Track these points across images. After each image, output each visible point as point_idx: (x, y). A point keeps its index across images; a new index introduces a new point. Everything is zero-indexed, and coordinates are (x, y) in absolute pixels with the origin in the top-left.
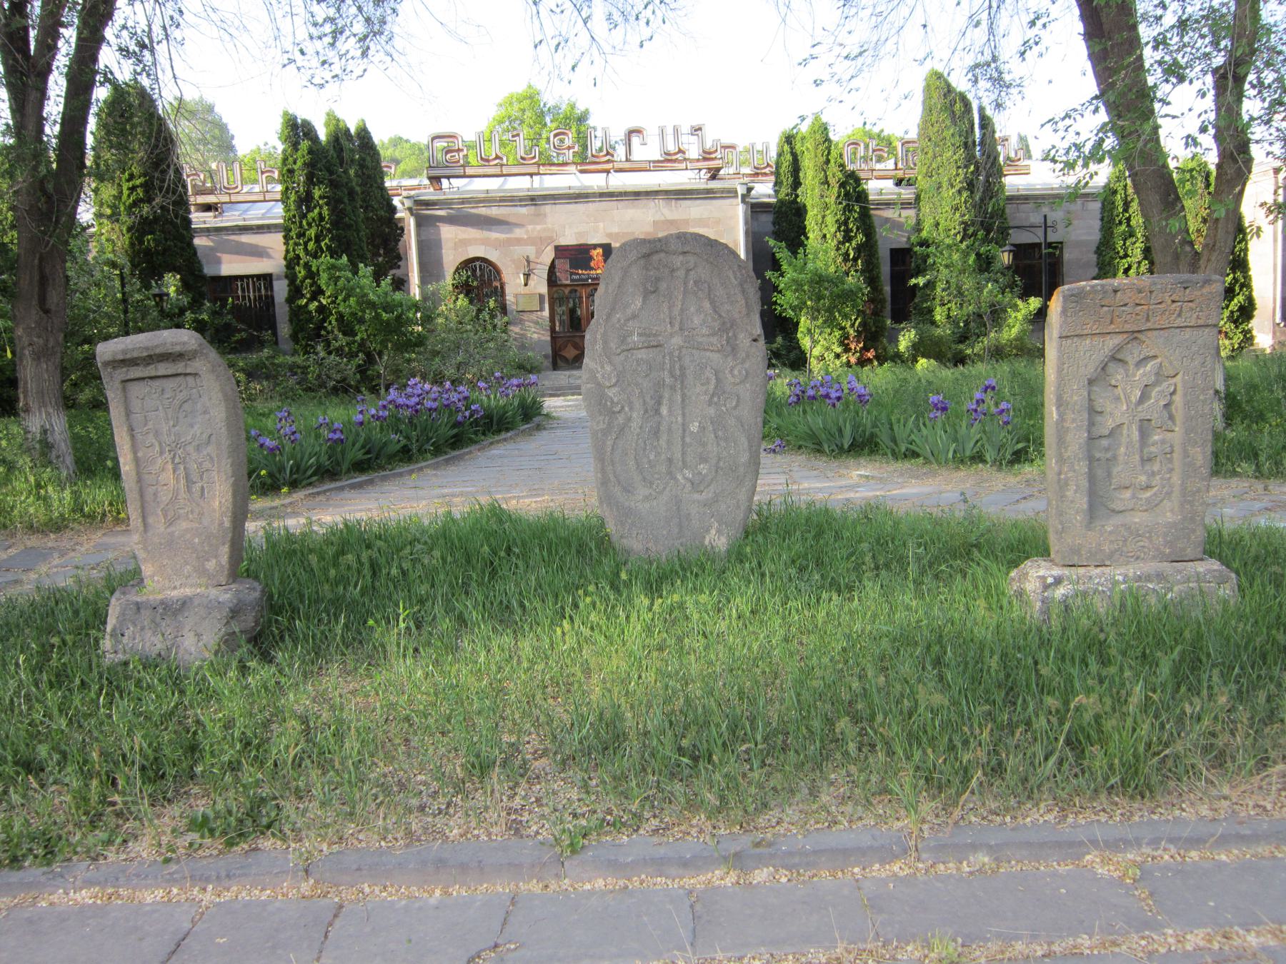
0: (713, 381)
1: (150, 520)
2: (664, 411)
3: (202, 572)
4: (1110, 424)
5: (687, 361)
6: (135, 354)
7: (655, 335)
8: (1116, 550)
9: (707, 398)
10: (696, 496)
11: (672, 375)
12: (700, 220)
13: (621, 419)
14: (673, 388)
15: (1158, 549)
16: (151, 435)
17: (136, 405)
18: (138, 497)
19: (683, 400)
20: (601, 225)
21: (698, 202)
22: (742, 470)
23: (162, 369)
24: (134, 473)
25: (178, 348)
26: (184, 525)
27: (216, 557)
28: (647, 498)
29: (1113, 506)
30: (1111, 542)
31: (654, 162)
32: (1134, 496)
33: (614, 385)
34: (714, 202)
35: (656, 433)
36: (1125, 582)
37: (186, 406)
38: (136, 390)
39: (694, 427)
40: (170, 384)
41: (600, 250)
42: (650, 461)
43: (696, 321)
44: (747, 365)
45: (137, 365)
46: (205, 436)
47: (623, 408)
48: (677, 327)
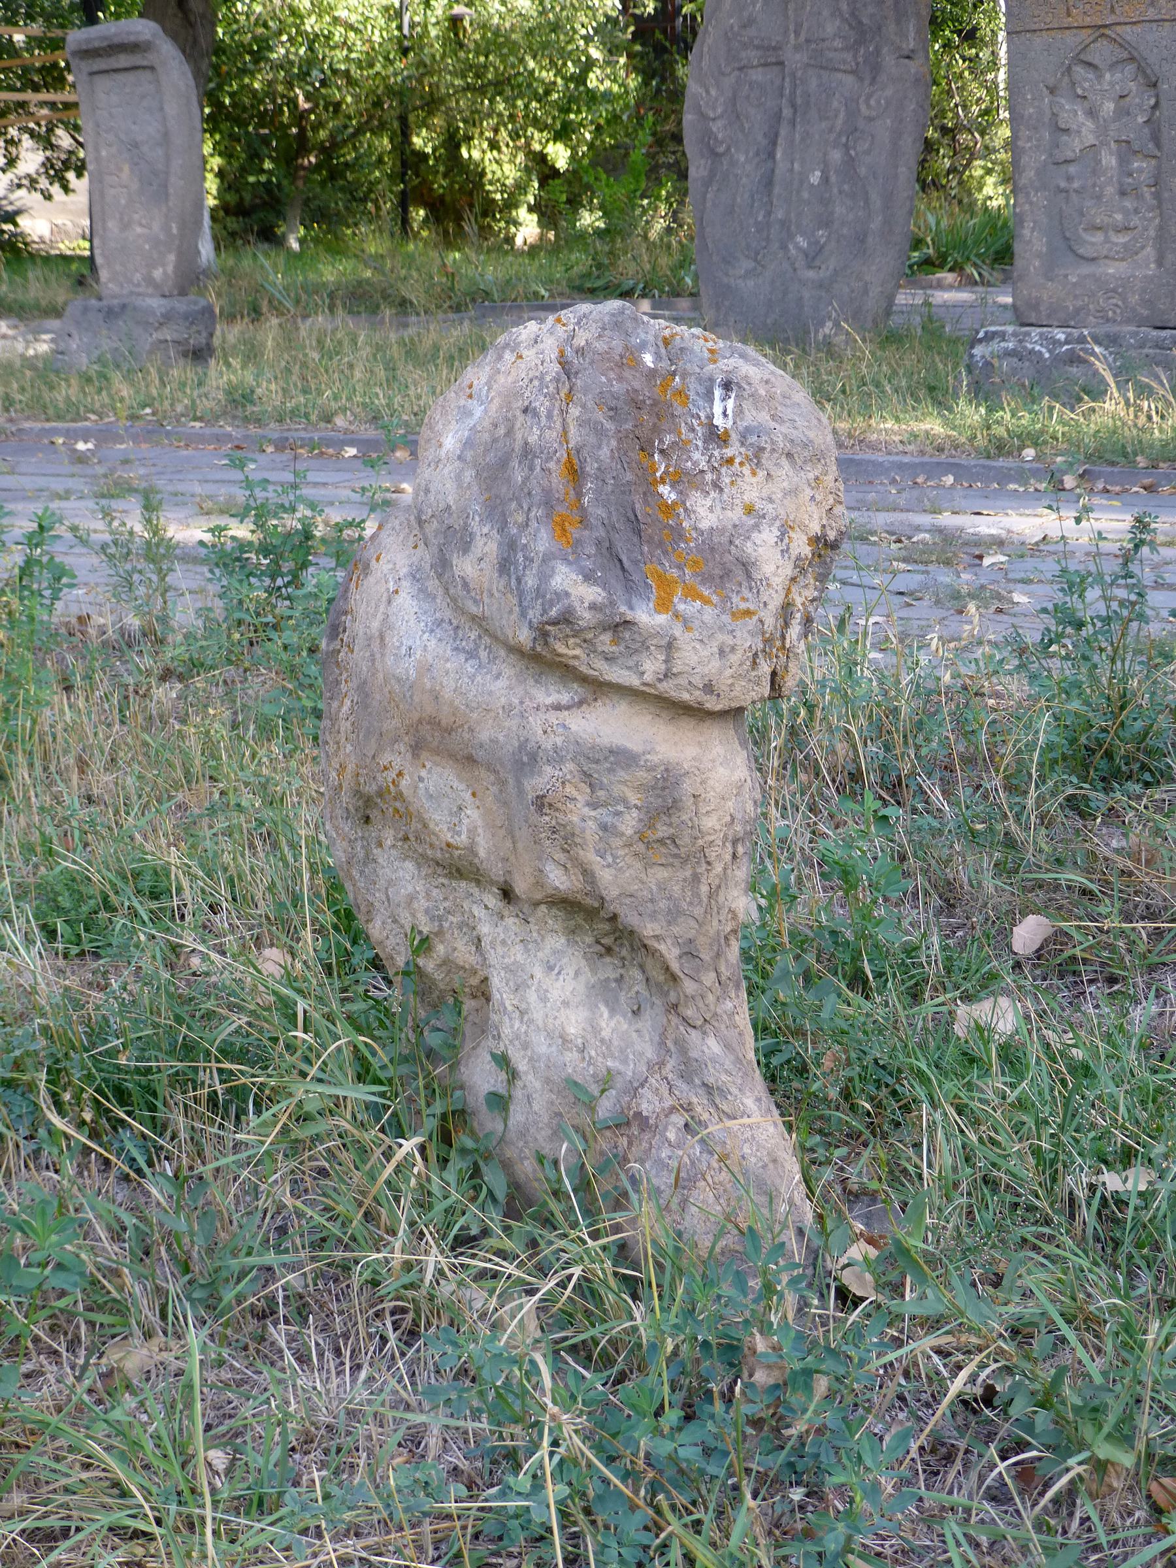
0: (842, 115)
2: (779, 155)
4: (1077, 145)
5: (813, 83)
6: (97, 44)
7: (775, 49)
8: (1082, 308)
9: (833, 136)
10: (811, 274)
11: (793, 106)
13: (725, 162)
14: (793, 123)
15: (1133, 310)
19: (803, 140)
22: (870, 239)
23: (123, 60)
25: (132, 38)
27: (164, 265)
28: (749, 274)
29: (1081, 251)
30: (1076, 297)
32: (1107, 240)
33: (721, 116)
35: (768, 182)
36: (1067, 342)
39: (815, 178)
40: (130, 77)
42: (756, 223)
43: (830, 28)
44: (889, 92)
47: (728, 149)
48: (802, 38)
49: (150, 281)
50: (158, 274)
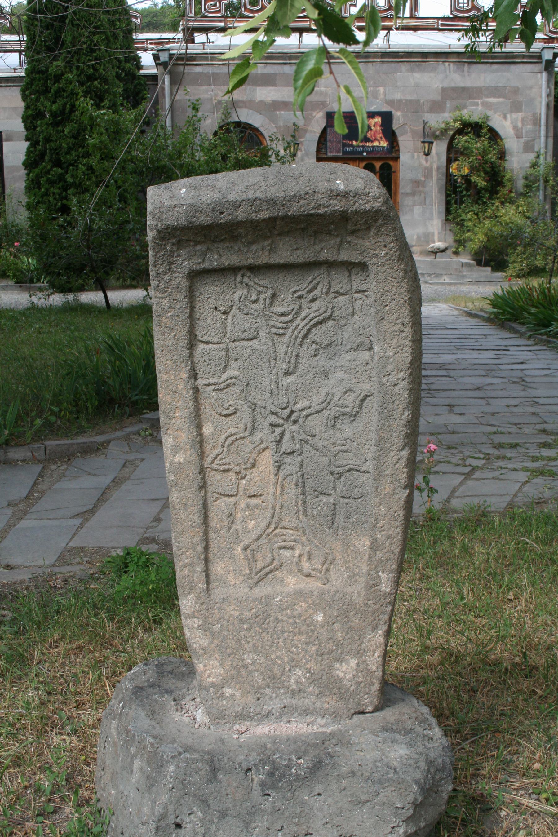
1: (218, 568)
3: (328, 685)
12: (496, 88)
16: (235, 390)
17: (209, 322)
18: (198, 520)
20: (382, 90)
21: (495, 67)
24: (192, 470)
25: (338, 205)
26: (293, 583)
27: (358, 653)
31: (444, 19)
34: (513, 67)
37: (318, 334)
38: (211, 294)
41: (378, 120)
45: (235, 238)
46: (351, 400)
49: (328, 685)
50: (346, 670)
